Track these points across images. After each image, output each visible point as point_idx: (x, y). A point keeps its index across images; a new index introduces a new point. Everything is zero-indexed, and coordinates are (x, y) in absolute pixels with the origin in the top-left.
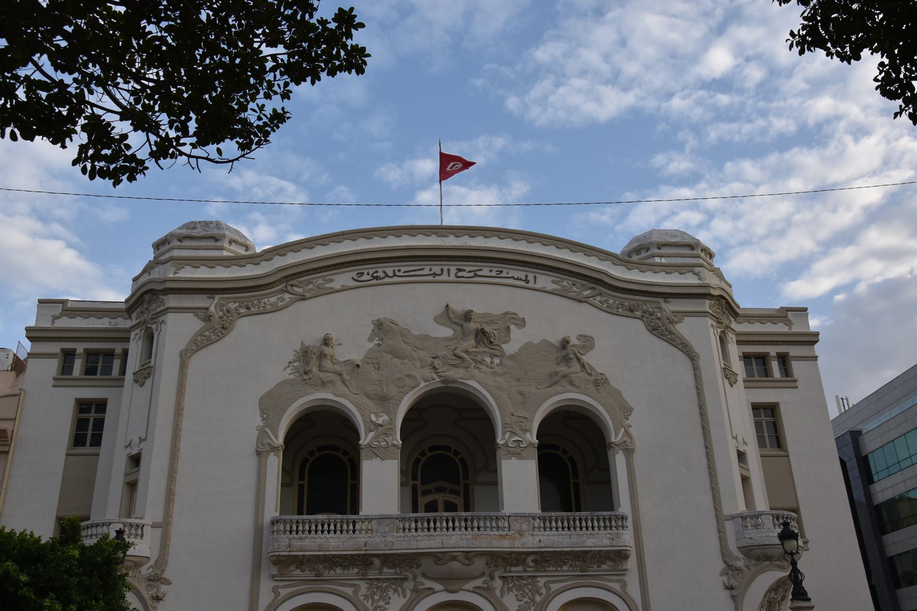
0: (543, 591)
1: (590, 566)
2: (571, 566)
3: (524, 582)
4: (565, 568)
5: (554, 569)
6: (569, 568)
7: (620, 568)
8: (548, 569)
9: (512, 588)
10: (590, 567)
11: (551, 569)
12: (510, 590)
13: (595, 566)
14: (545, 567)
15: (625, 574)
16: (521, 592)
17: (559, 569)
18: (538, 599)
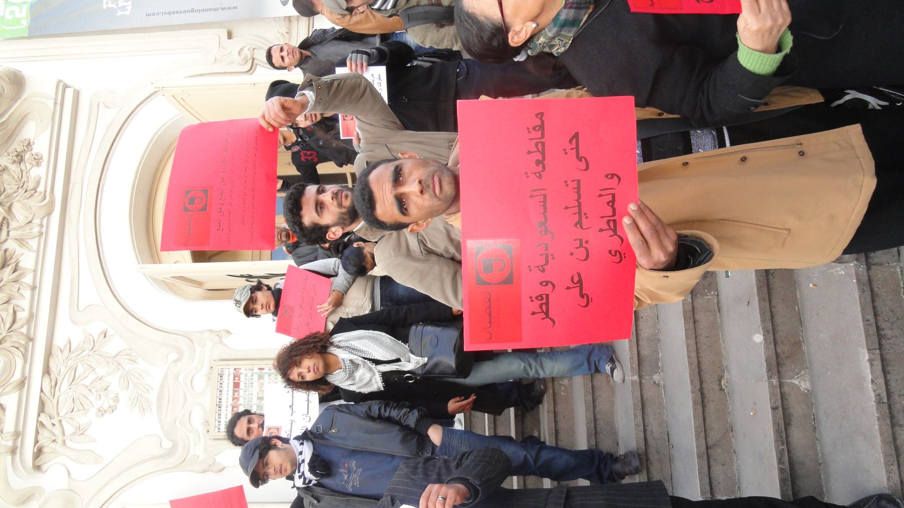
0: (96, 329)
1: (31, 185)
2: (21, 241)
3: (65, 385)
4: (27, 260)
5: (27, 293)
6: (30, 249)
7: (51, 104)
8: (22, 316)
9: (79, 428)
10: (35, 189)
11: (25, 304)
12: (80, 431)
13: (38, 172)
14: (14, 321)
15: (77, 95)
16: (92, 398)
17: (28, 279)
18: (112, 347)
